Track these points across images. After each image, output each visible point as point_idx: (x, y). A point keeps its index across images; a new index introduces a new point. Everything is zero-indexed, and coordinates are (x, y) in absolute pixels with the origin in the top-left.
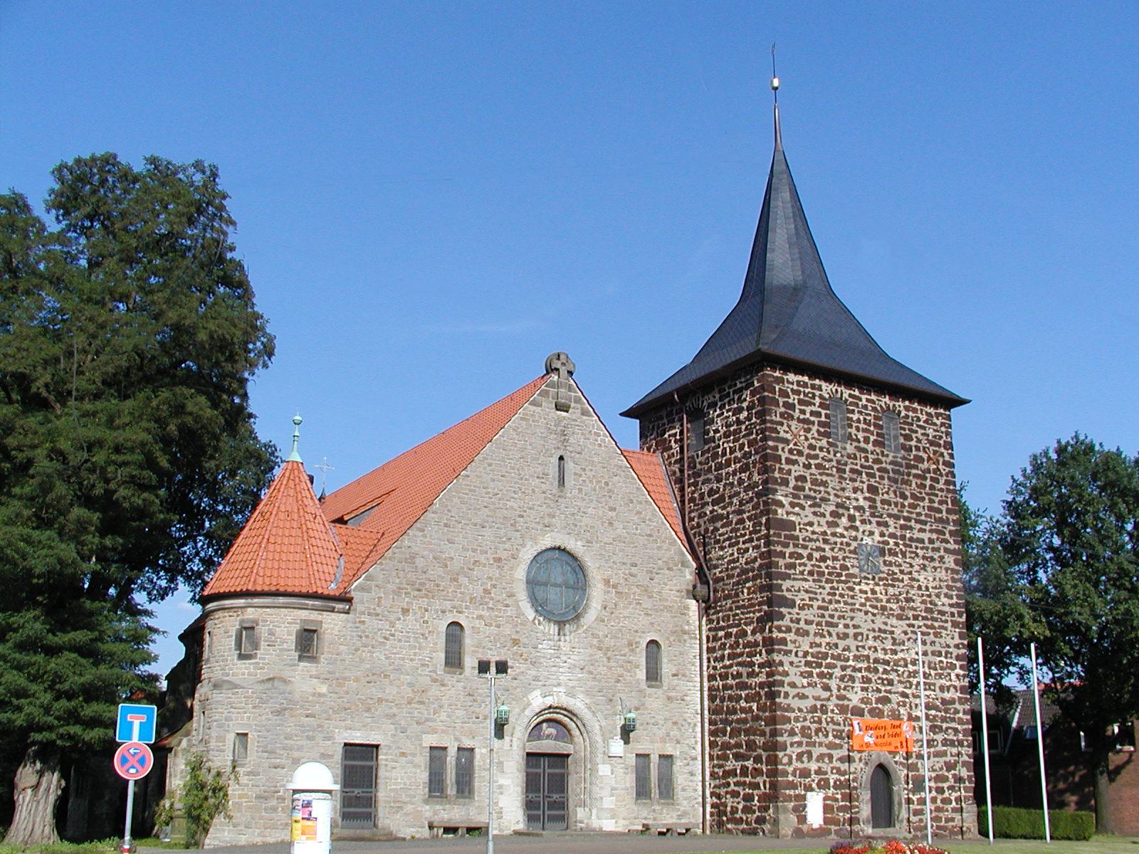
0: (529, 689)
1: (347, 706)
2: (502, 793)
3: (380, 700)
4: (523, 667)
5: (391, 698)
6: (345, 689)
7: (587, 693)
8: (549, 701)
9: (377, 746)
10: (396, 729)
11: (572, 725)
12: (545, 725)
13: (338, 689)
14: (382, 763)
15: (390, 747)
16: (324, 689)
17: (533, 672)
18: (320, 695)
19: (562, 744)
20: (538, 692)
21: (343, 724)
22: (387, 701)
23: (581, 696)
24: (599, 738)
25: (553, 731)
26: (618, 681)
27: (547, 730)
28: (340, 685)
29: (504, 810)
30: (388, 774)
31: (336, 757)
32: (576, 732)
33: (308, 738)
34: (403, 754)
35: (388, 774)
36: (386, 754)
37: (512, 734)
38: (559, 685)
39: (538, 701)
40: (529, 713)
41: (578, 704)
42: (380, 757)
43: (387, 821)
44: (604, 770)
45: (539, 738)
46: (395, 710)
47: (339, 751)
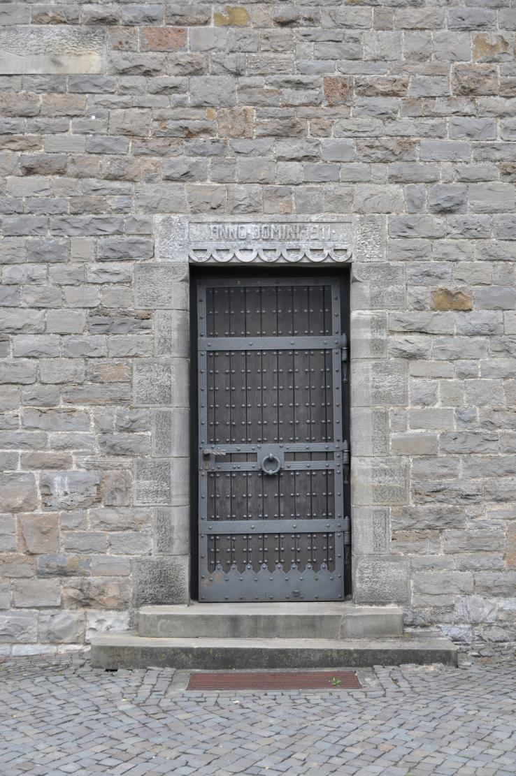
1: (196, 120)
3: (340, 92)
5: (380, 77)
6: (183, 56)
9: (340, 274)
10: (415, 204)
13: (148, 59)
14: (361, 335)
15: (389, 273)
16: (93, 60)
18: (80, 85)
21: (183, 191)
22: (367, 90)
28: (161, 44)
30: (387, 382)
31: (156, 321)
33: (38, 257)
34: (452, 301)
35: (387, 382)
36: (375, 301)
42: (354, 314)
43: (394, 573)
46: (406, 125)
47: (176, 294)
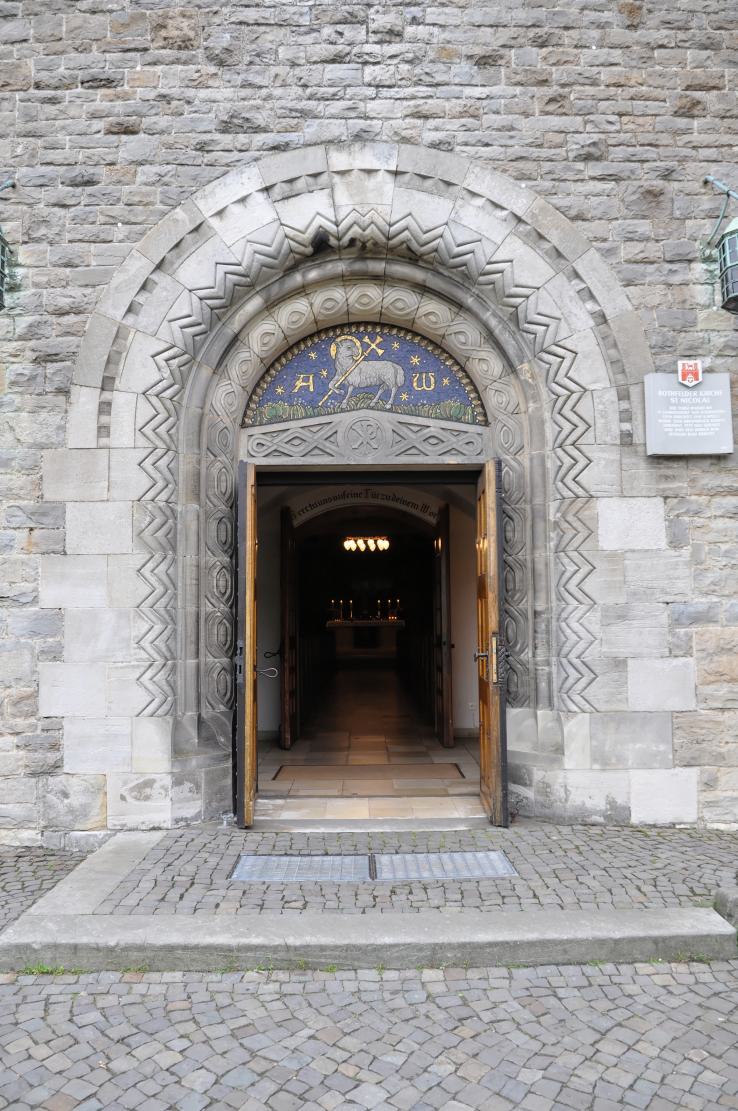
0: (205, 159)
2: (55, 655)
4: (171, 78)
7: (518, 168)
8: (308, 214)
11: (464, 335)
12: (343, 349)
17: (223, 94)
19: (435, 426)
20: (247, 180)
23: (487, 183)
24: (591, 371)
25: (388, 372)
26: (689, 111)
27: (355, 362)
29: (70, 733)
32: (487, 366)
37: (107, 383)
38: (361, 137)
39: (246, 220)
40: (200, 272)
41: (474, 220)
44: (629, 522)
45: (313, 404)
